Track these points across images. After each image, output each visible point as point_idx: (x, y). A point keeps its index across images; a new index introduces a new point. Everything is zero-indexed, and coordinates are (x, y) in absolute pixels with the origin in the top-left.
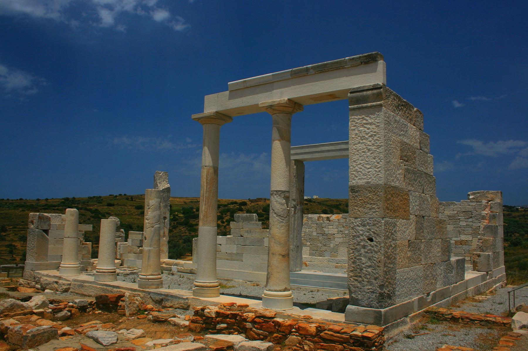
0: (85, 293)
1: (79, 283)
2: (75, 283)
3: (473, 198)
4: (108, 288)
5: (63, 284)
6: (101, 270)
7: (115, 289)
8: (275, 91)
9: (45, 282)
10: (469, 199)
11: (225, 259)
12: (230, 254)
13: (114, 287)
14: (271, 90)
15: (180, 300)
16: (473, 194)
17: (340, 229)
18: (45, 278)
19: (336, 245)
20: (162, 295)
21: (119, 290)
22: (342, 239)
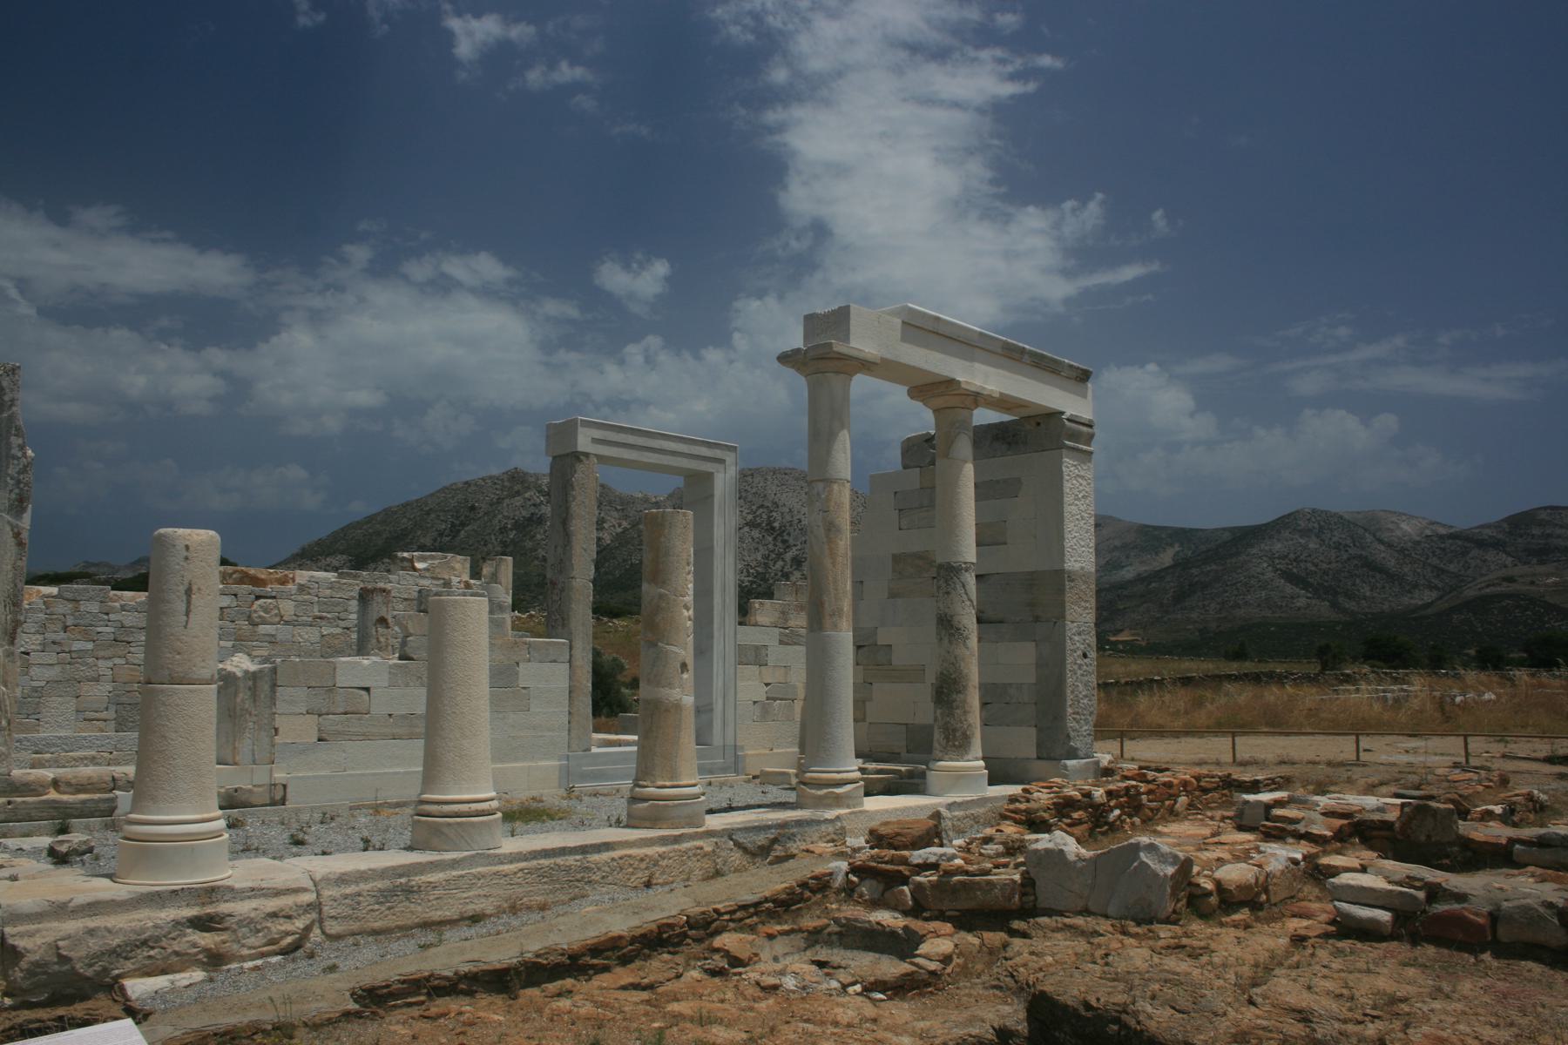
0: (437, 915)
1: (380, 884)
2: (348, 891)
3: (427, 570)
4: (559, 860)
5: (274, 915)
6: (474, 806)
7: (595, 857)
8: (977, 365)
9: (94, 945)
10: (415, 569)
11: (384, 737)
12: (403, 717)
13: (584, 850)
14: (972, 359)
15: (823, 827)
16: (423, 559)
17: (51, 636)
18: (72, 926)
19: (35, 690)
20: (769, 827)
21: (616, 854)
22: (58, 669)
